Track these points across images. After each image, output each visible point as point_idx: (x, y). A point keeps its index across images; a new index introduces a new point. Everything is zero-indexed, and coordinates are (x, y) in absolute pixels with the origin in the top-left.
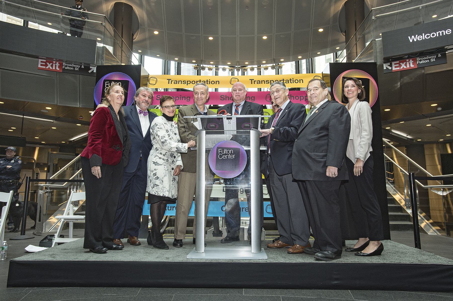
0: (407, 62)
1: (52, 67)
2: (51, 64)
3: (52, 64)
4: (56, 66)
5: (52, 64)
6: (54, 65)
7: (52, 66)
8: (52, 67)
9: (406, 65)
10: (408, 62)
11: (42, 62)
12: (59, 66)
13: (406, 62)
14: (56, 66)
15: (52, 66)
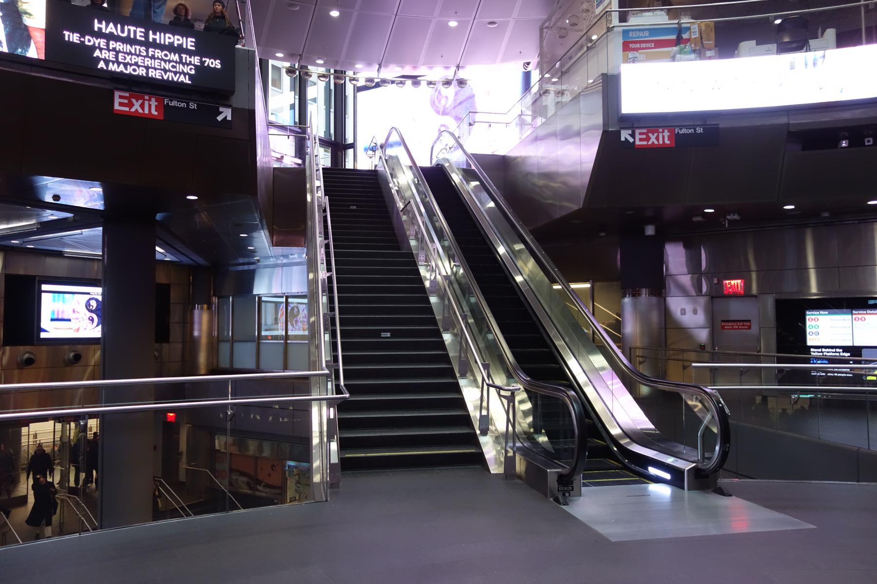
0: (660, 134)
1: (143, 108)
2: (140, 102)
3: (142, 101)
4: (150, 106)
5: (142, 101)
6: (146, 103)
7: (142, 106)
8: (143, 108)
9: (657, 139)
10: (661, 134)
11: (121, 97)
12: (156, 105)
13: (659, 133)
14: (150, 106)
15: (142, 106)
